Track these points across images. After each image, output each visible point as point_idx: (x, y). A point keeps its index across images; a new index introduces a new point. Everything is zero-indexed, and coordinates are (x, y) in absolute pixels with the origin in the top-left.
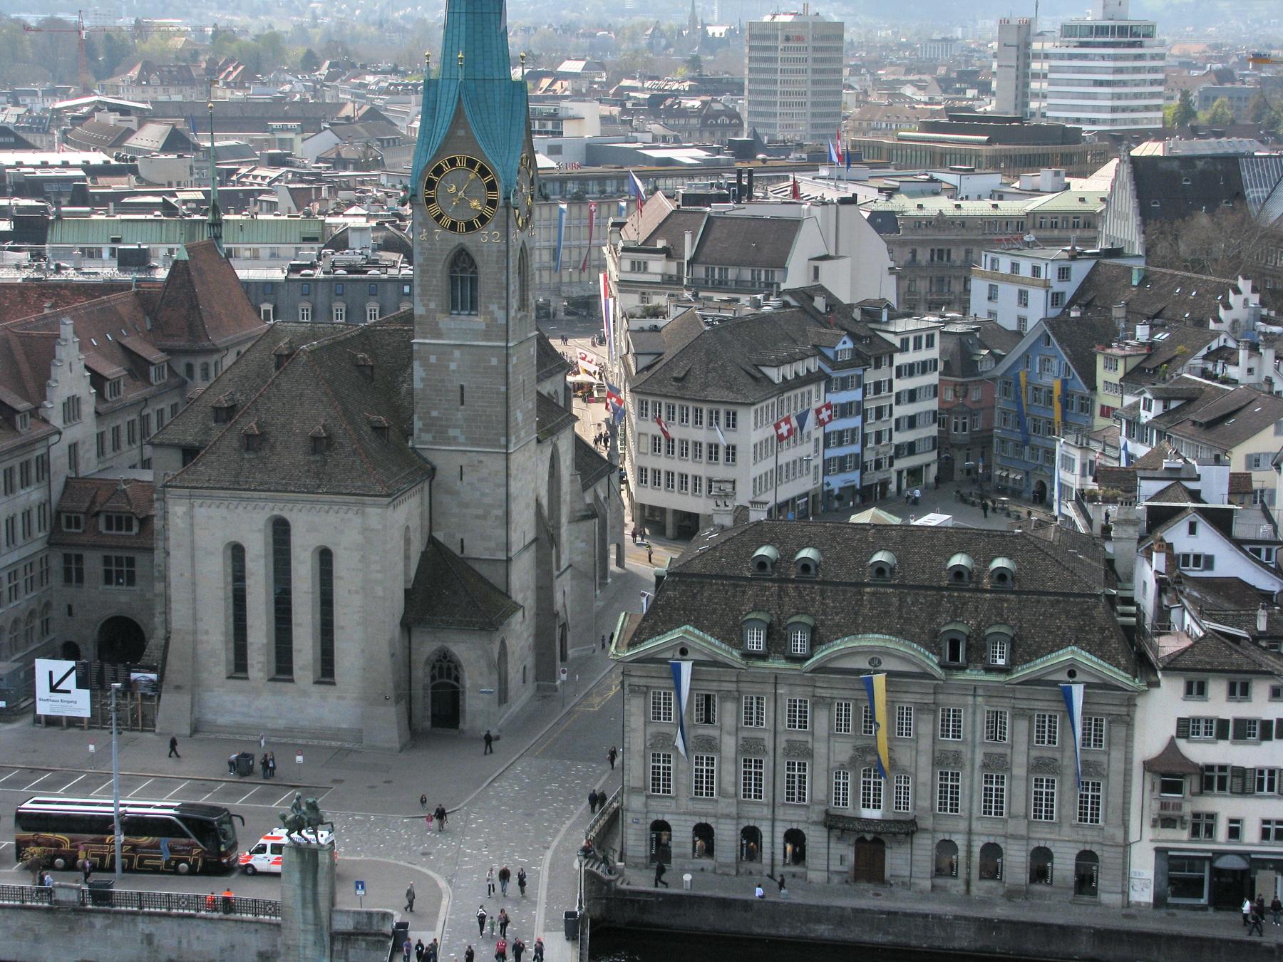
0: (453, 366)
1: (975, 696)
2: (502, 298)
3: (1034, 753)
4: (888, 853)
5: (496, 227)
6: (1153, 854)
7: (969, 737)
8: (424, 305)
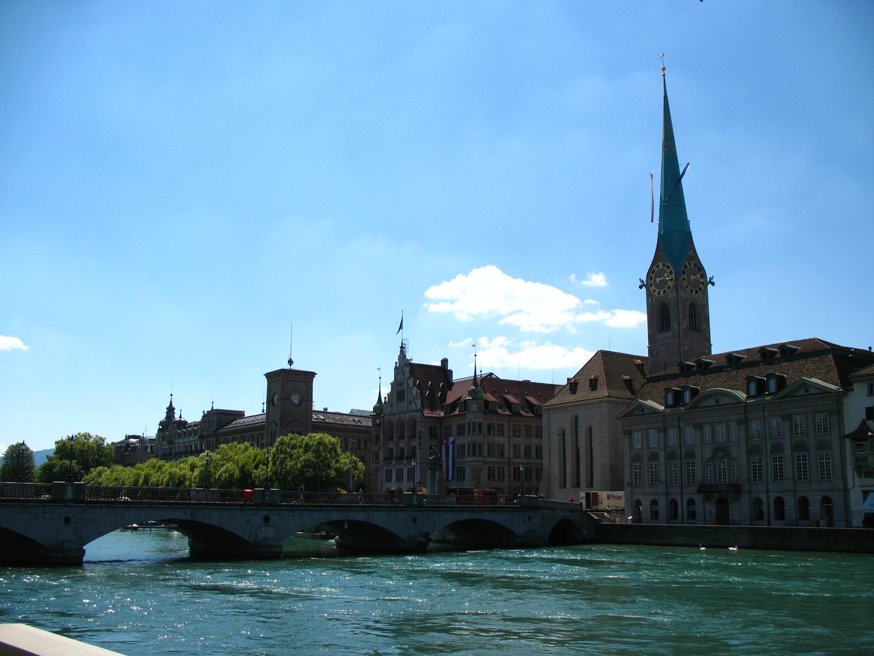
0: (661, 354)
1: (763, 412)
4: (730, 506)
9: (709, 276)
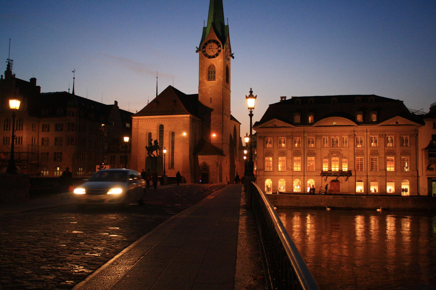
0: (209, 93)
2: (222, 74)
3: (386, 149)
5: (220, 56)
6: (427, 180)
7: (366, 146)
8: (202, 78)
9: (232, 53)
